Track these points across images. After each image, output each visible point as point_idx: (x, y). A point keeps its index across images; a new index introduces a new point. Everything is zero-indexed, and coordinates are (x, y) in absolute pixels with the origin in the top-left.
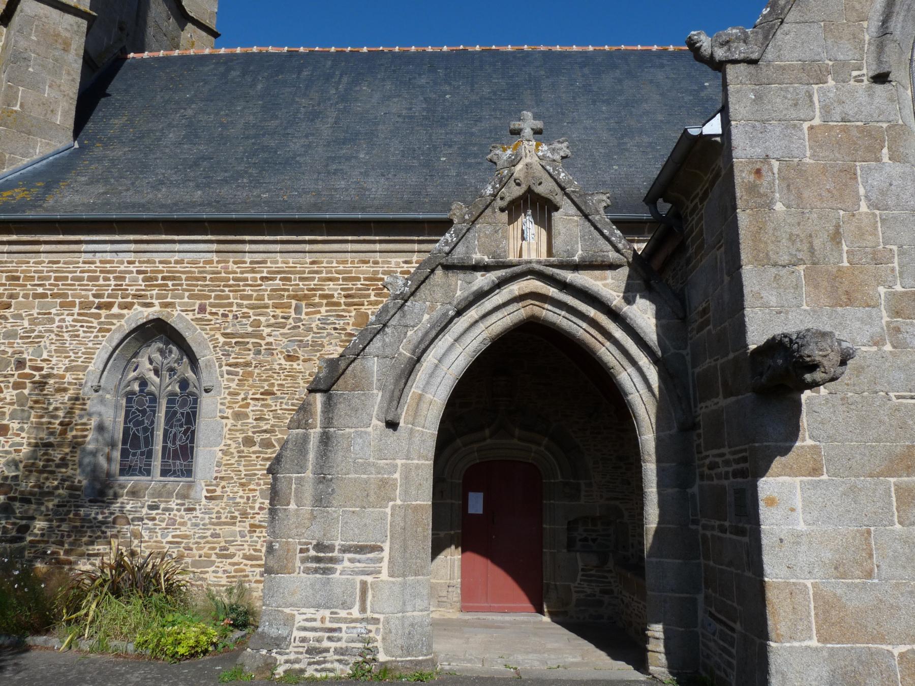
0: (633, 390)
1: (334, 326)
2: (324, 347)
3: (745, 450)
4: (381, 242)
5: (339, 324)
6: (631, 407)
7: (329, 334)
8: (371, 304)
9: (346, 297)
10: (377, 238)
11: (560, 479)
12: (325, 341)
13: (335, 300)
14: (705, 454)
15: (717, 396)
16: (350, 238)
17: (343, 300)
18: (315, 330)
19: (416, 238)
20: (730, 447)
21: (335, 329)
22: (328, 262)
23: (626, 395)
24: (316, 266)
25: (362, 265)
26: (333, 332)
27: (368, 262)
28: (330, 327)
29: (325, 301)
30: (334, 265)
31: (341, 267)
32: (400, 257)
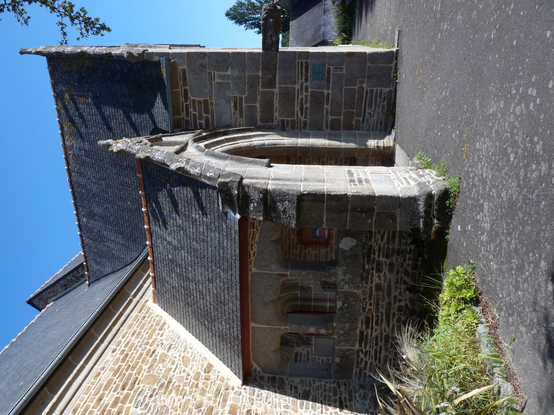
0: (263, 142)
1: (148, 397)
2: (165, 406)
3: (298, 62)
4: (86, 362)
5: (147, 393)
6: (270, 145)
7: (155, 401)
8: (139, 373)
9: (123, 389)
10: (82, 362)
11: (299, 292)
12: (159, 404)
13: (122, 397)
14: (296, 118)
15: (273, 93)
16: (69, 379)
17: (125, 391)
18: (146, 411)
19: (97, 341)
20: (295, 84)
21: (151, 396)
22: (81, 401)
23: (264, 145)
24: (79, 409)
25: (100, 377)
26: (153, 398)
27: (99, 374)
28: (147, 400)
29: (120, 404)
30: (86, 396)
31: (93, 391)
32: (108, 354)
